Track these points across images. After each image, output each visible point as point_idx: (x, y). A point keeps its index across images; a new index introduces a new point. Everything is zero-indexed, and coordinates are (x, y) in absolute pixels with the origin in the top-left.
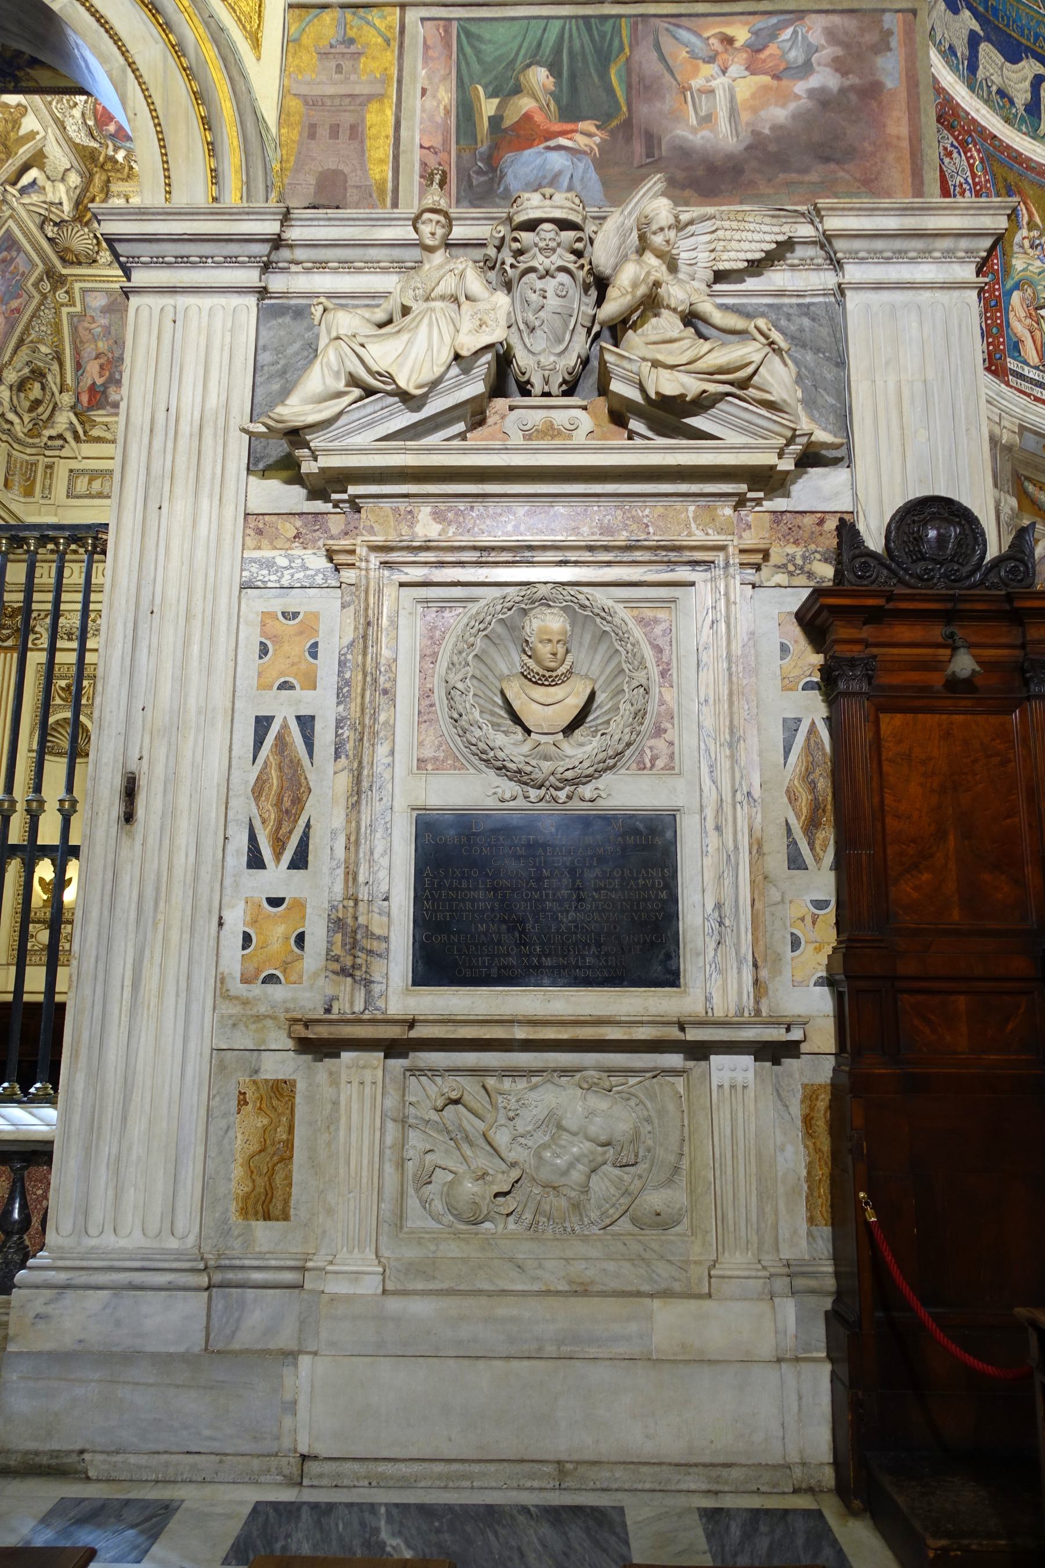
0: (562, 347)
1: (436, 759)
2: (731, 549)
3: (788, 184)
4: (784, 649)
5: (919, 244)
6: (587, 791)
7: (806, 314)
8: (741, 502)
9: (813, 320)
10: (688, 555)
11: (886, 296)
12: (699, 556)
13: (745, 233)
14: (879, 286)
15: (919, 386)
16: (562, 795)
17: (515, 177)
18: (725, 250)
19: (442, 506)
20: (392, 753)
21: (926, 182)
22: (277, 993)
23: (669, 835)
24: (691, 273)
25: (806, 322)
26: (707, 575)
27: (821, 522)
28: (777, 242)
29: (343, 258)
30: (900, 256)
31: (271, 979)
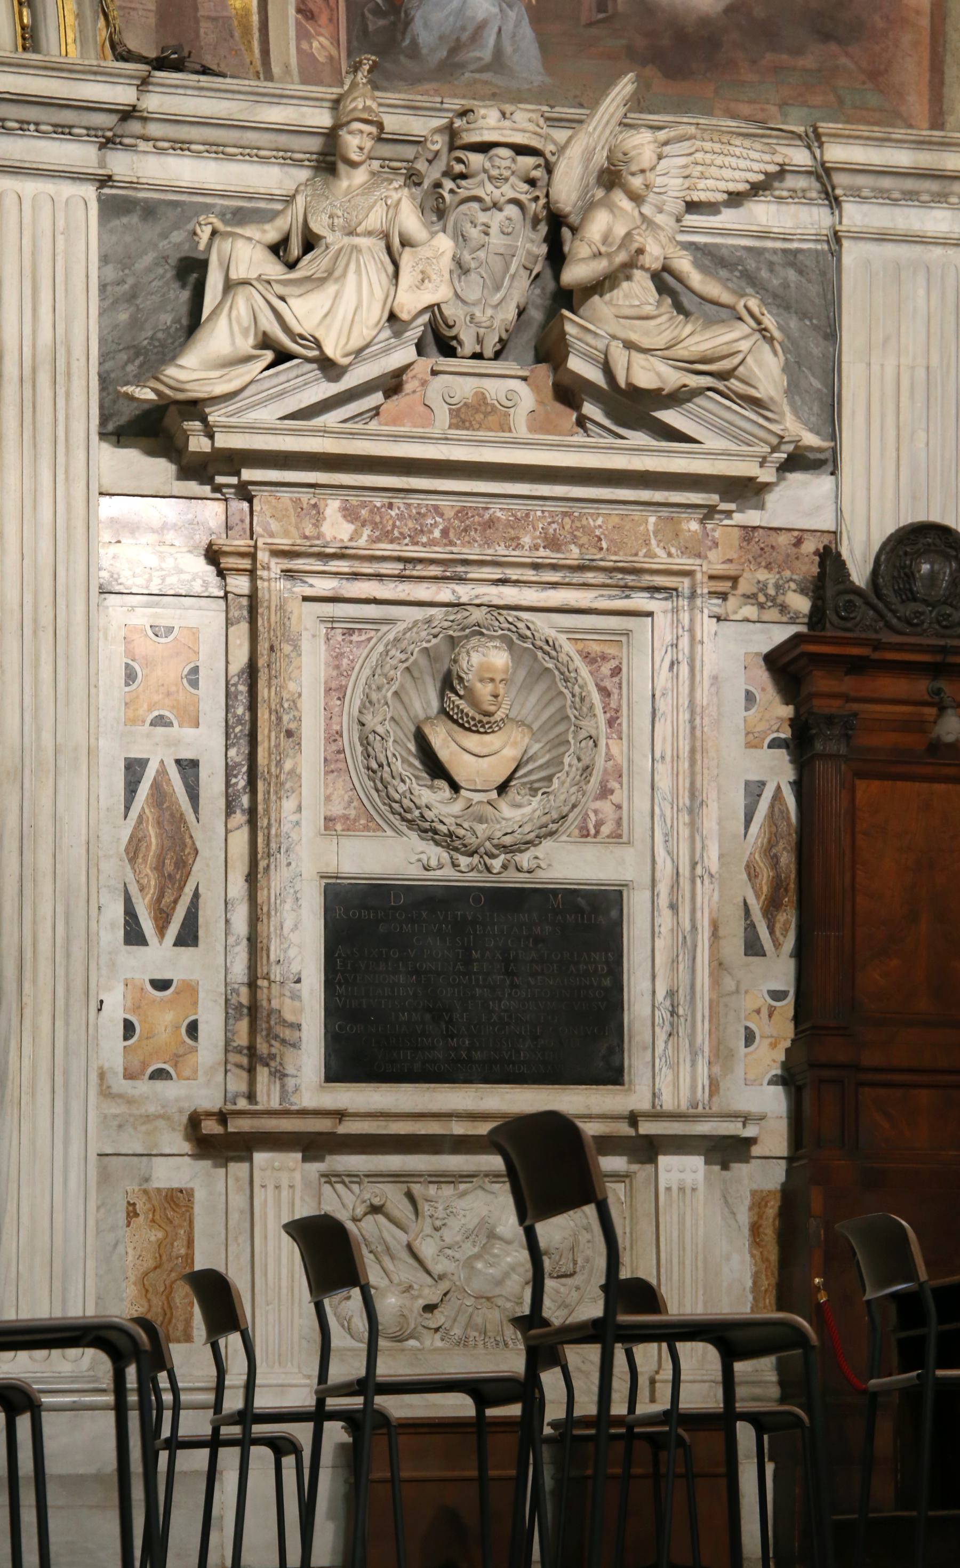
0: (498, 296)
1: (346, 818)
2: (699, 576)
3: (777, 69)
4: (750, 698)
5: (934, 186)
6: (524, 859)
7: (792, 264)
8: (710, 512)
9: (801, 272)
10: (648, 580)
11: (890, 250)
12: (660, 581)
13: (729, 159)
14: (882, 237)
15: (921, 373)
16: (496, 864)
17: (426, 25)
18: (703, 176)
19: (354, 501)
20: (299, 809)
21: (948, 80)
22: (169, 1090)
23: (614, 914)
24: (659, 204)
25: (792, 275)
26: (668, 605)
27: (798, 542)
28: (766, 174)
29: (211, 140)
30: (911, 196)
31: (160, 1075)
